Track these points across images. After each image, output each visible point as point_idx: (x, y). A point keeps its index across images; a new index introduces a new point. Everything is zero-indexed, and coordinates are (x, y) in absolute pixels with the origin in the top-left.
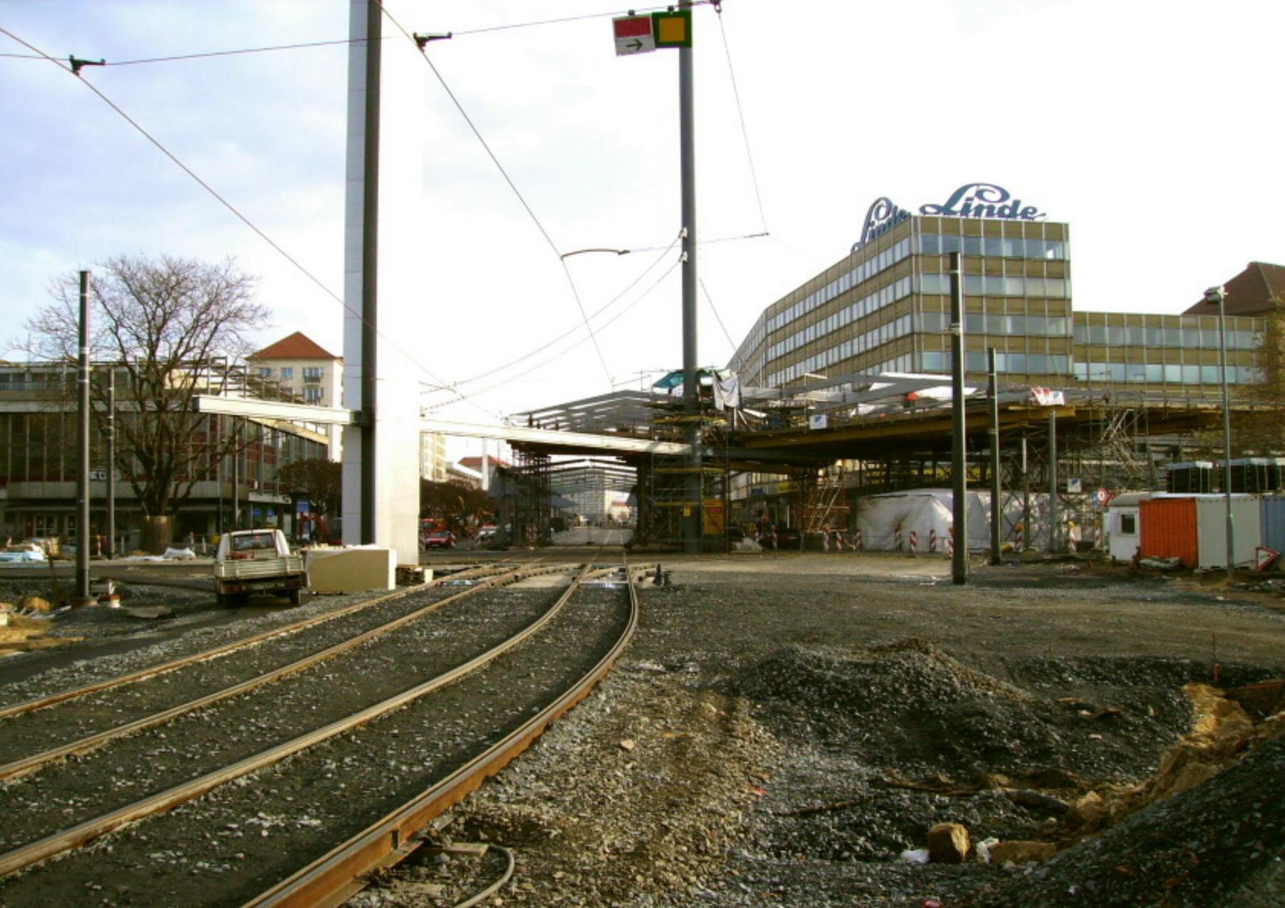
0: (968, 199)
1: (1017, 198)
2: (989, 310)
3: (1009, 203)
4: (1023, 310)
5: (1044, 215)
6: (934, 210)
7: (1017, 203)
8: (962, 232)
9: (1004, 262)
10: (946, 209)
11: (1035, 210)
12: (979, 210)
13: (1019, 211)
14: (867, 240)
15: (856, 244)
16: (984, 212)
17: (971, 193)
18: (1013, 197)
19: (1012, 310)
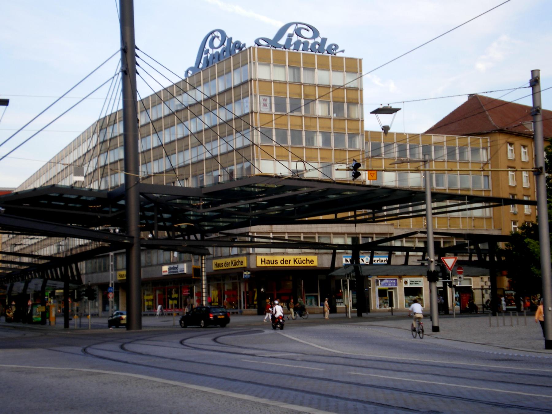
0: (290, 36)
1: (325, 37)
3: (319, 40)
4: (330, 128)
5: (343, 51)
6: (265, 43)
7: (324, 40)
9: (317, 87)
10: (273, 43)
11: (337, 47)
12: (298, 43)
13: (326, 48)
14: (201, 66)
15: (191, 69)
16: (302, 46)
17: (291, 30)
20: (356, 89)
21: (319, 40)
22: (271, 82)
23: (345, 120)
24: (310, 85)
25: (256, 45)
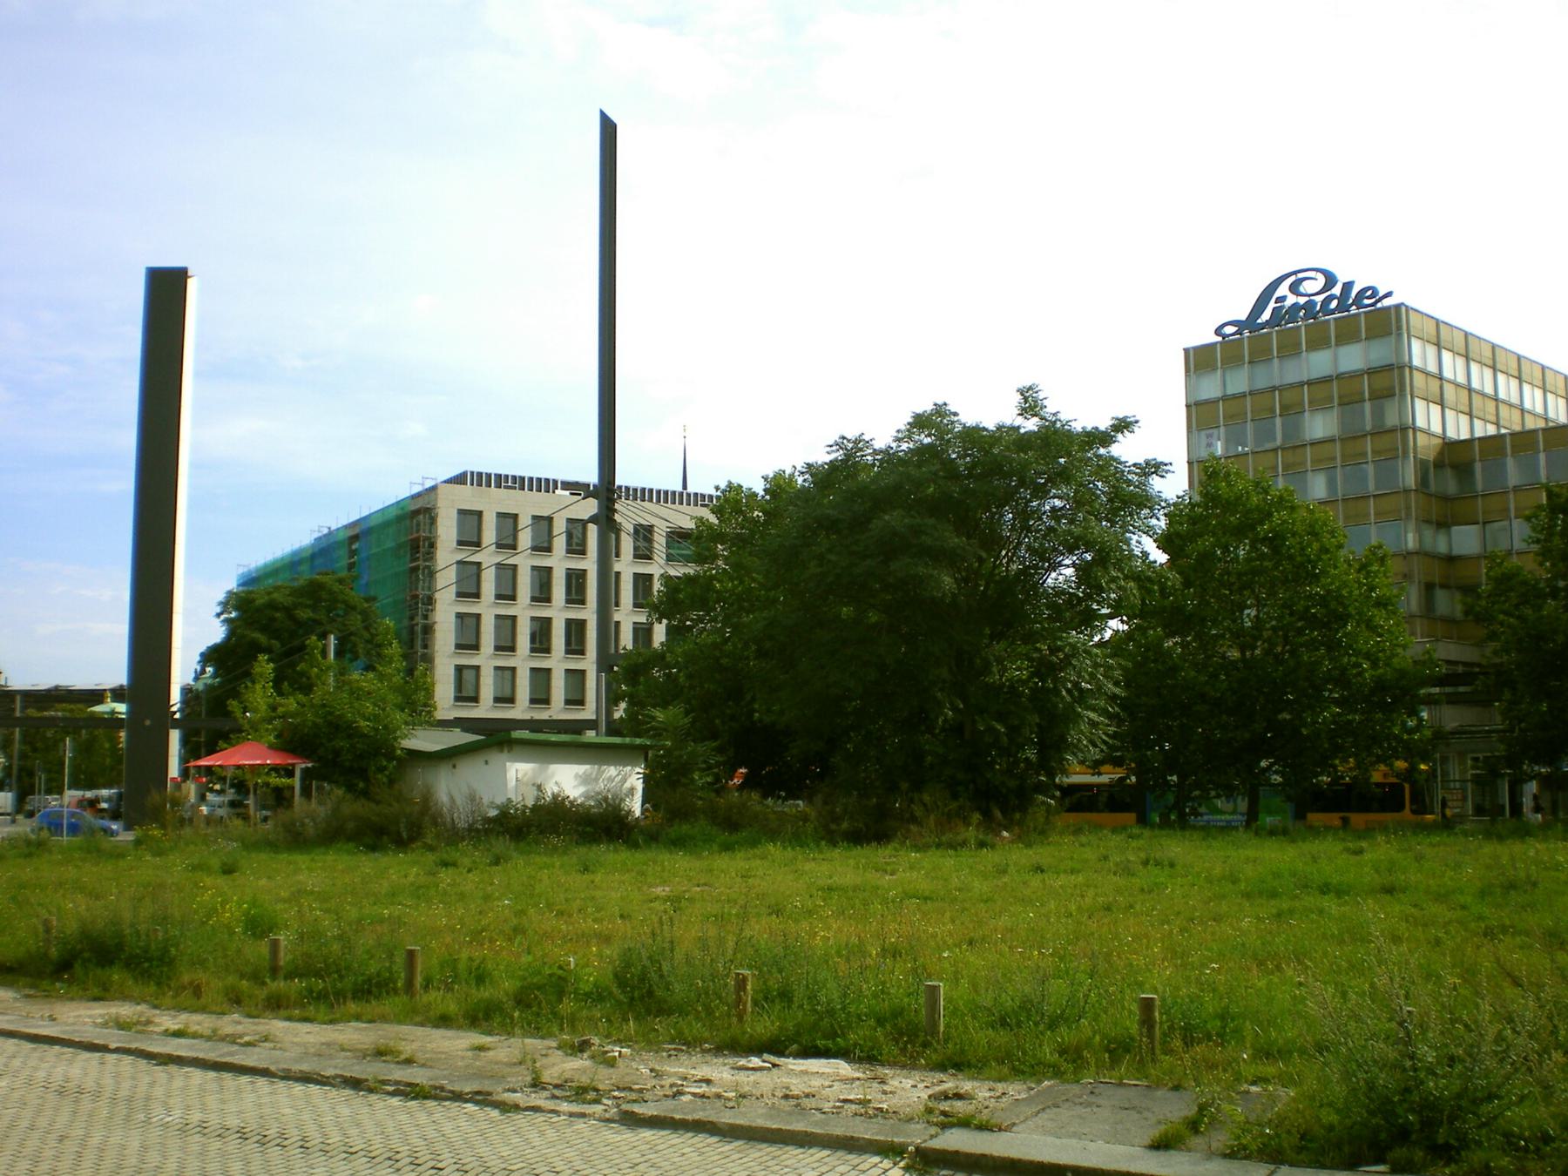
2: (1286, 467)
4: (1334, 459)
7: (1348, 286)
8: (1247, 359)
10: (1250, 323)
17: (1283, 290)
18: (1343, 278)
19: (1320, 461)
20: (1389, 368)
21: (1337, 290)
24: (1292, 386)
25: (1220, 339)
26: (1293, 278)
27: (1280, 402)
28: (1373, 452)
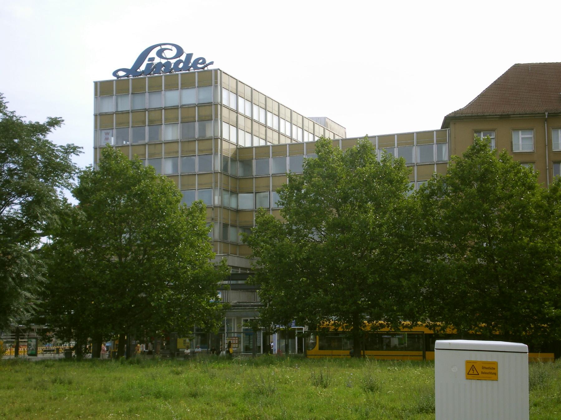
4: (178, 152)
7: (189, 56)
8: (130, 92)
10: (133, 71)
17: (153, 54)
19: (169, 153)
20: (210, 104)
21: (183, 58)
22: (113, 114)
23: (195, 141)
24: (155, 109)
25: (115, 78)
26: (159, 48)
27: (149, 117)
28: (199, 150)
